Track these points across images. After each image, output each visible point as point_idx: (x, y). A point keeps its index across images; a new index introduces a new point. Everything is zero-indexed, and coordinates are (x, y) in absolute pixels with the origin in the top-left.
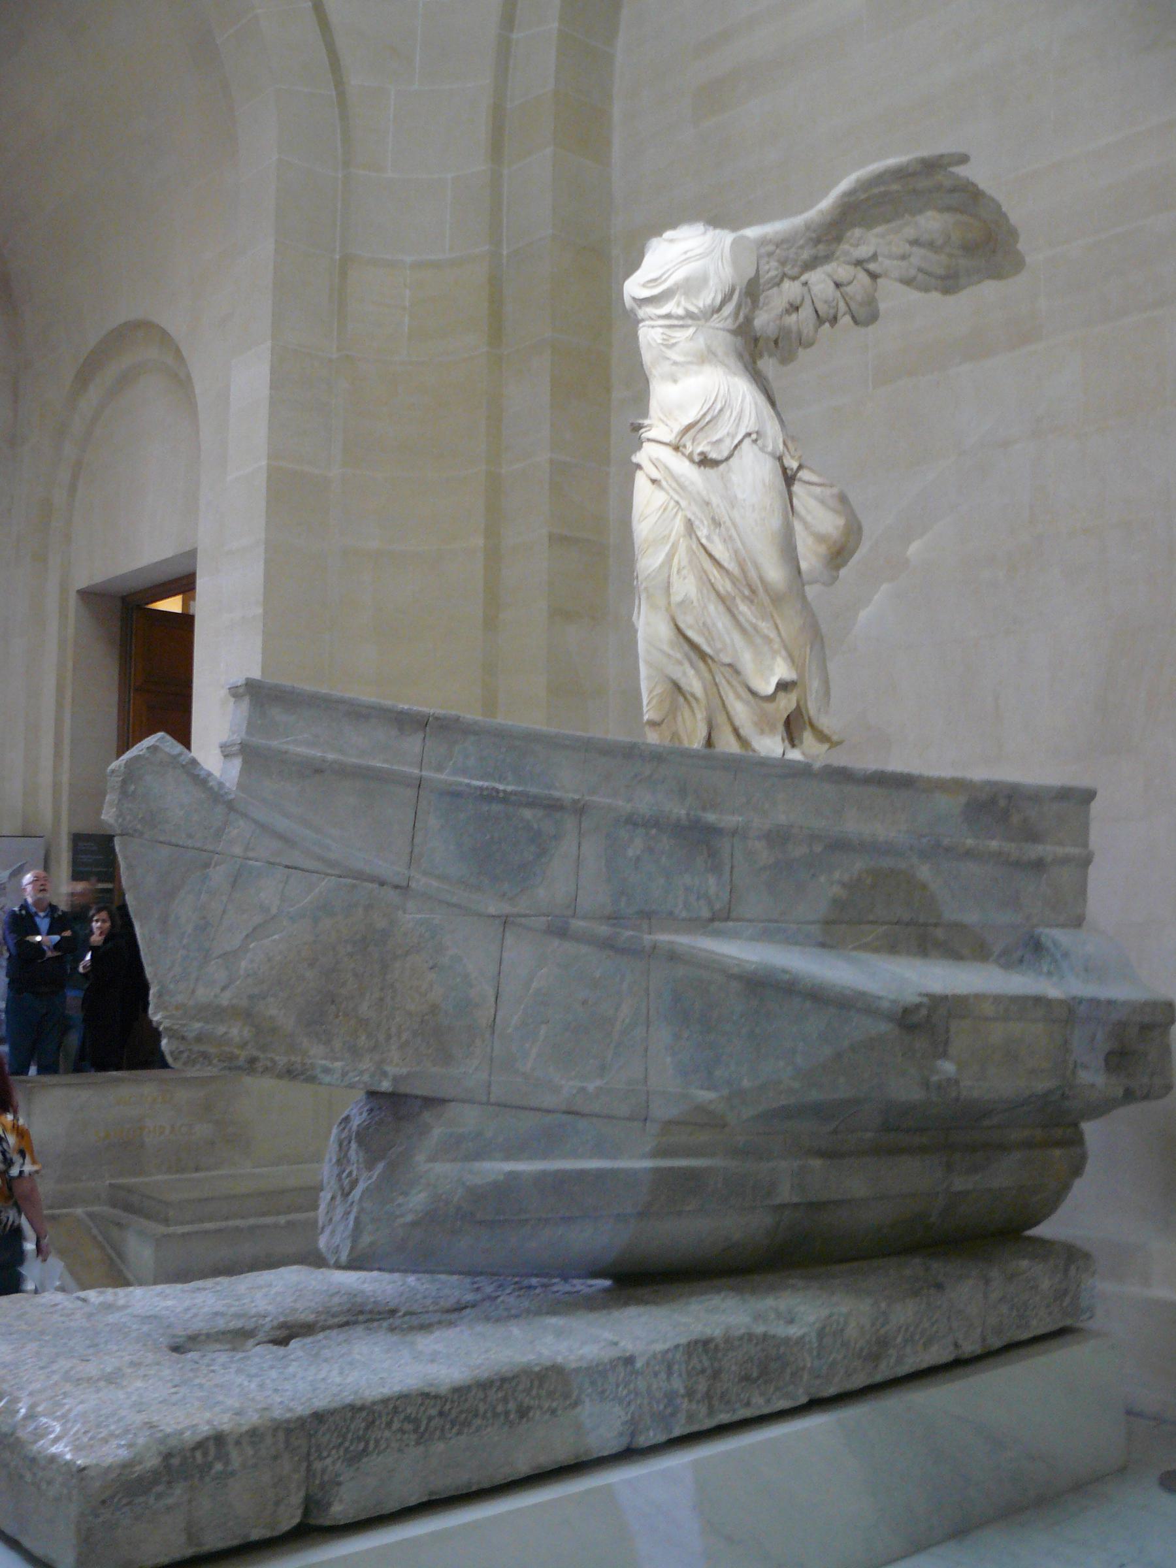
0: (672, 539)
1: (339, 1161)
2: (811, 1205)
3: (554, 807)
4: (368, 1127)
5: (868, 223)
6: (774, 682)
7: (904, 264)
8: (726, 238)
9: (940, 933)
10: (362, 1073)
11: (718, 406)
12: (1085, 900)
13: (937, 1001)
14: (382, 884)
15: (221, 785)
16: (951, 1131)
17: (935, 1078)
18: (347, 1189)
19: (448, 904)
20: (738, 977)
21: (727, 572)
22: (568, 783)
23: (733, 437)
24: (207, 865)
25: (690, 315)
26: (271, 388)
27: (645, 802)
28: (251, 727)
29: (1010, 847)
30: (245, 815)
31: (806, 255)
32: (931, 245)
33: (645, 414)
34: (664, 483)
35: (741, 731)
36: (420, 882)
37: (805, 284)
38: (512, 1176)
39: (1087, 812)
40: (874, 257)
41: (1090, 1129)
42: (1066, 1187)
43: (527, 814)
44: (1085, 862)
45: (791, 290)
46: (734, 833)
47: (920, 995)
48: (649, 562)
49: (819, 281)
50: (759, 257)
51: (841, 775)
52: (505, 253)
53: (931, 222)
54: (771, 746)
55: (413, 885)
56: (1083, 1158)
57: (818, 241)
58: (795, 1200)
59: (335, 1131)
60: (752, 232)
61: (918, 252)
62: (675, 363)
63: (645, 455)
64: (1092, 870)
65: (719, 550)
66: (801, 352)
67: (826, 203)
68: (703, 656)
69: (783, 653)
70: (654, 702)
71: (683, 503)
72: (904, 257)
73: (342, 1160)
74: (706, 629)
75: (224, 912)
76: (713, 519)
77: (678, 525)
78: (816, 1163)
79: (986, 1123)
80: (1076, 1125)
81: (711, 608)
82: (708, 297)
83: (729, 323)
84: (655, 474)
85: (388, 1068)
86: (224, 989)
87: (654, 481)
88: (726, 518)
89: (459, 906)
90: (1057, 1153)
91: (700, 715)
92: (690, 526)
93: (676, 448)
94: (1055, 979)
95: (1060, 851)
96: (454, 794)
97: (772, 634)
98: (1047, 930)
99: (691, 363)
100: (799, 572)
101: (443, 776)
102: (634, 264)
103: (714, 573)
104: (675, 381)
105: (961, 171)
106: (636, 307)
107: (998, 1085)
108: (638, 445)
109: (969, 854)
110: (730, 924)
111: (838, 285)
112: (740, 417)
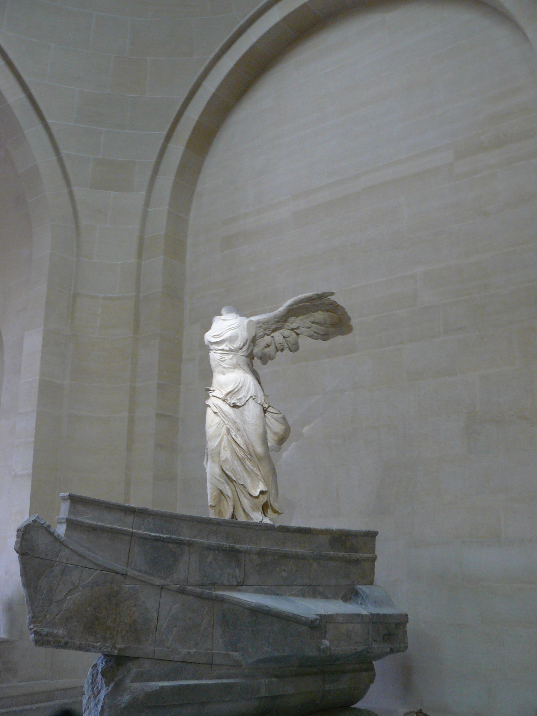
0: (221, 435)
1: (92, 683)
2: (272, 697)
3: (180, 543)
4: (106, 669)
5: (297, 315)
6: (259, 491)
7: (309, 330)
8: (246, 321)
9: (320, 589)
10: (108, 647)
11: (240, 385)
12: (374, 574)
13: (323, 617)
14: (117, 573)
15: (59, 535)
16: (326, 667)
17: (322, 647)
18: (96, 694)
19: (142, 581)
21: (242, 448)
22: (185, 534)
23: (246, 397)
24: (52, 567)
25: (231, 350)
26: (43, 346)
27: (213, 541)
28: (70, 512)
29: (346, 554)
30: (67, 547)
31: (273, 327)
32: (319, 324)
33: (210, 384)
34: (219, 414)
35: (246, 510)
36: (132, 572)
37: (272, 337)
38: (163, 688)
39: (375, 541)
40: (298, 328)
41: (376, 664)
42: (368, 687)
43: (171, 546)
44: (374, 559)
45: (267, 339)
46: (246, 552)
47: (316, 615)
48: (212, 444)
49: (278, 336)
50: (257, 328)
51: (285, 529)
52: (141, 296)
53: (320, 316)
54: (257, 517)
55: (129, 574)
56: (374, 675)
57: (278, 322)
58: (267, 695)
59: (90, 670)
60: (254, 318)
62: (224, 368)
63: (211, 402)
64: (377, 563)
65: (239, 440)
66: (270, 361)
67: (282, 309)
68: (232, 480)
69: (262, 480)
70: (213, 498)
71: (226, 422)
72: (309, 328)
73: (94, 682)
74: (234, 471)
75: (58, 585)
76: (237, 428)
77: (224, 430)
78: (275, 680)
79: (338, 663)
80: (371, 663)
81: (236, 462)
82: (238, 344)
83: (246, 354)
84: (216, 410)
85: (117, 645)
86: (56, 615)
87: (215, 413)
88: (242, 428)
89: (145, 582)
90: (364, 674)
91: (231, 504)
92: (228, 430)
93: (224, 401)
94: (363, 606)
95: (365, 555)
96: (145, 539)
97: (258, 473)
98: (360, 587)
99: (230, 368)
100: (268, 447)
101: (141, 532)
102: (207, 327)
103: (237, 449)
104: (224, 374)
105: (332, 298)
107: (344, 648)
108: (208, 397)
109: (331, 558)
110: (244, 587)
111: (284, 337)
112: (248, 390)
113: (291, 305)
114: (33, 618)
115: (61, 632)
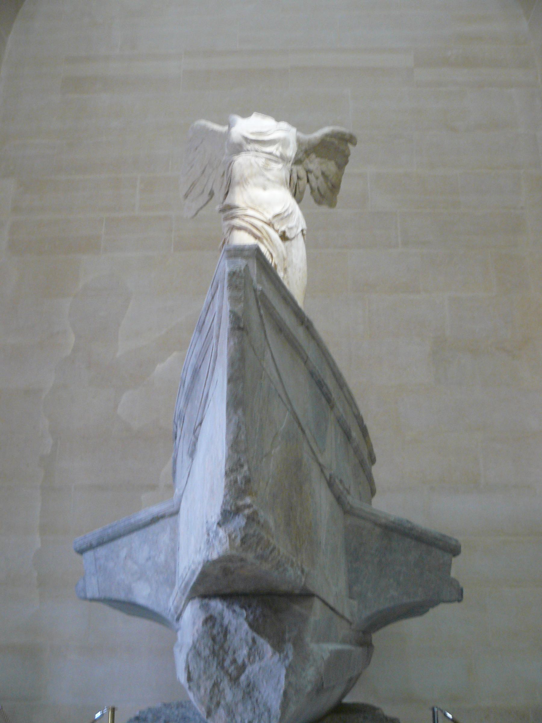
1: (214, 653)
11: (290, 211)
20: (380, 525)
23: (298, 229)
34: (265, 241)
53: (331, 167)
61: (321, 179)
62: (268, 180)
71: (274, 255)
106: (244, 142)
111: (298, 178)
113: (327, 135)
114: (248, 480)
115: (272, 523)
